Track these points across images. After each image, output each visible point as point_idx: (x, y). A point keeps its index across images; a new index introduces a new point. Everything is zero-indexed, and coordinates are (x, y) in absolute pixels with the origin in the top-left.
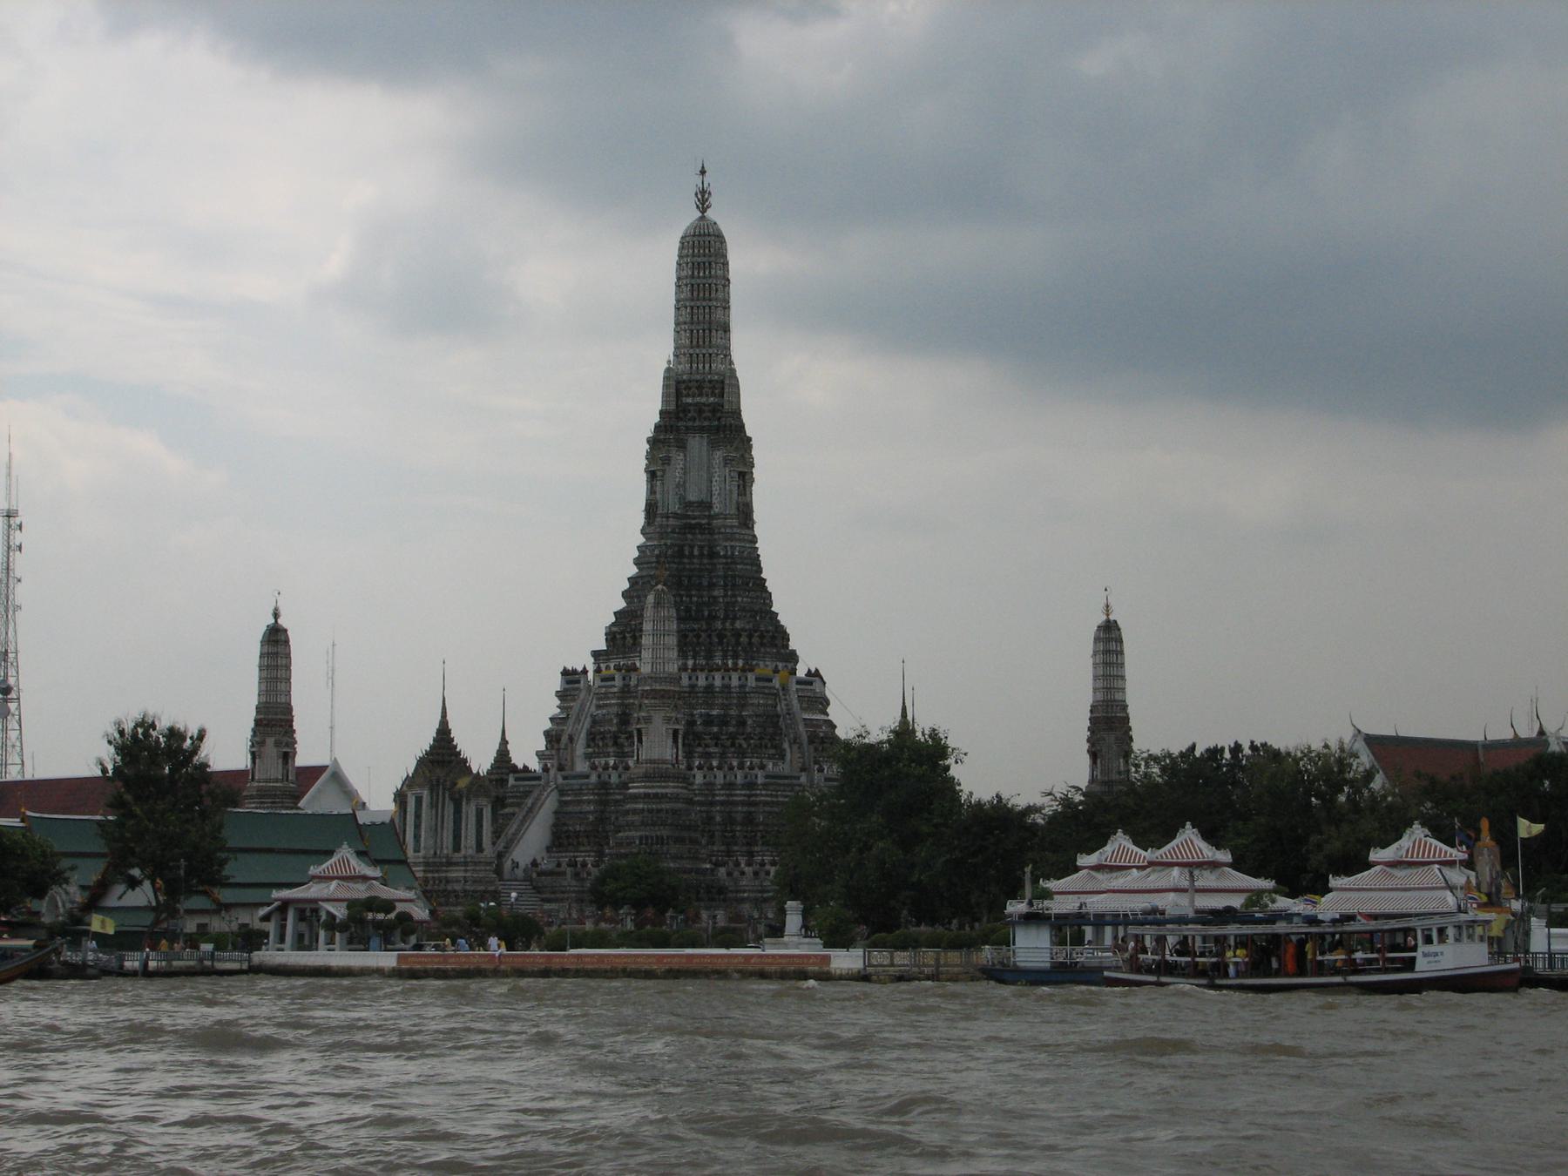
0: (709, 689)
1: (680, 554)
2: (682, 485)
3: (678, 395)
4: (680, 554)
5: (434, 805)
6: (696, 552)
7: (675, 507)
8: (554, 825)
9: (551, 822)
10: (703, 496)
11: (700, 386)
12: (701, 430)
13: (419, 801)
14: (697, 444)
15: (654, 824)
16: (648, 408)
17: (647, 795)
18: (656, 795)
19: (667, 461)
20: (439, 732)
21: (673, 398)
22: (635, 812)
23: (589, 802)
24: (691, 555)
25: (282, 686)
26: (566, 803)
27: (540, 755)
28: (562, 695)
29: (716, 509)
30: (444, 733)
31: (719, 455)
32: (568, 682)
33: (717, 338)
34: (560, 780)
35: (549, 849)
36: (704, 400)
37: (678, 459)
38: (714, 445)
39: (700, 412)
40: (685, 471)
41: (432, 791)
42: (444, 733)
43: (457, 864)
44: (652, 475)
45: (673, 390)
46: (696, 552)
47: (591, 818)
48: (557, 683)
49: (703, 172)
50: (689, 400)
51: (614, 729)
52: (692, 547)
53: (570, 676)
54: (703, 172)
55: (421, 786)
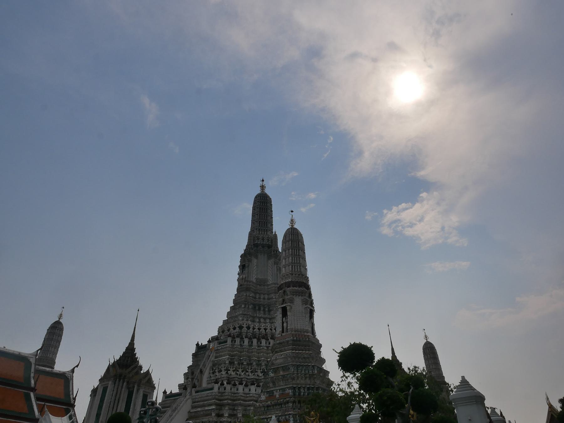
16: (241, 244)
19: (250, 261)
20: (127, 349)
27: (180, 386)
28: (194, 356)
30: (130, 350)
31: (271, 262)
33: (269, 225)
34: (194, 393)
37: (255, 261)
42: (130, 350)
44: (243, 267)
49: (263, 181)
53: (200, 348)
54: (263, 181)
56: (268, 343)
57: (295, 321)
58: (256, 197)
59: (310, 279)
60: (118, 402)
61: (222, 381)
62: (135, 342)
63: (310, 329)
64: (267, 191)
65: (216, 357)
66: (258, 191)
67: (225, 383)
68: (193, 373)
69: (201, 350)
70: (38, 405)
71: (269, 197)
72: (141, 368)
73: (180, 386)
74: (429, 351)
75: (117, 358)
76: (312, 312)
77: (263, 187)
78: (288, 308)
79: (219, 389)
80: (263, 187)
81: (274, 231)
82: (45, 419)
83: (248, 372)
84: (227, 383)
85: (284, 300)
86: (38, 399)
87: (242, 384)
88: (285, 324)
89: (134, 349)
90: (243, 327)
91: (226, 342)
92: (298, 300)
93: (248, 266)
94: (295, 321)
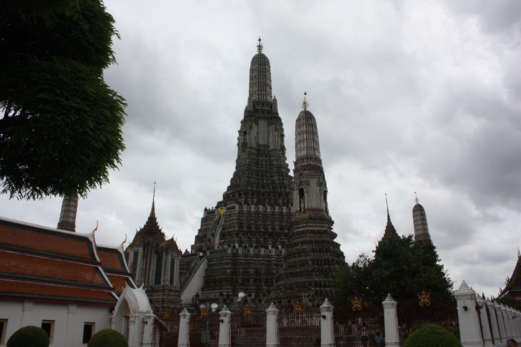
0: (281, 213)
1: (257, 163)
2: (257, 138)
3: (254, 106)
4: (257, 163)
5: (144, 256)
6: (264, 163)
7: (254, 145)
8: (205, 276)
9: (204, 275)
10: (266, 143)
11: (263, 104)
12: (264, 118)
13: (136, 255)
14: (263, 124)
15: (320, 251)
17: (313, 232)
18: (319, 232)
19: (251, 127)
20: (150, 219)
21: (252, 106)
22: (303, 243)
23: (227, 264)
24: (262, 164)
25: (72, 215)
26: (211, 265)
29: (272, 147)
30: (152, 219)
31: (272, 127)
32: (208, 213)
33: (268, 89)
35: (203, 289)
36: (264, 108)
38: (269, 125)
39: (263, 112)
40: (258, 133)
41: (144, 248)
42: (152, 219)
43: (158, 291)
45: (252, 103)
47: (228, 271)
48: (201, 215)
49: (260, 40)
50: (259, 108)
51: (237, 229)
52: (262, 162)
54: (260, 40)
55: (138, 246)
56: (273, 209)
57: (311, 201)
58: (253, 59)
59: (323, 162)
60: (150, 264)
61: (234, 245)
62: (156, 211)
63: (324, 208)
64: (264, 52)
65: (225, 221)
66: (256, 52)
67: (237, 245)
68: (205, 236)
69: (209, 213)
70: (107, 276)
71: (267, 58)
72: (163, 235)
73: (192, 247)
74: (419, 211)
75: (143, 227)
76: (325, 192)
77: (260, 47)
78: (305, 190)
79: (232, 250)
80: (260, 47)
81: (273, 95)
82: (127, 291)
83: (256, 235)
84: (239, 246)
85: (301, 182)
86: (106, 271)
87: (252, 246)
88: (302, 205)
89: (155, 219)
90: (248, 193)
91: (234, 208)
92: (313, 182)
93: (249, 133)
94: (311, 201)
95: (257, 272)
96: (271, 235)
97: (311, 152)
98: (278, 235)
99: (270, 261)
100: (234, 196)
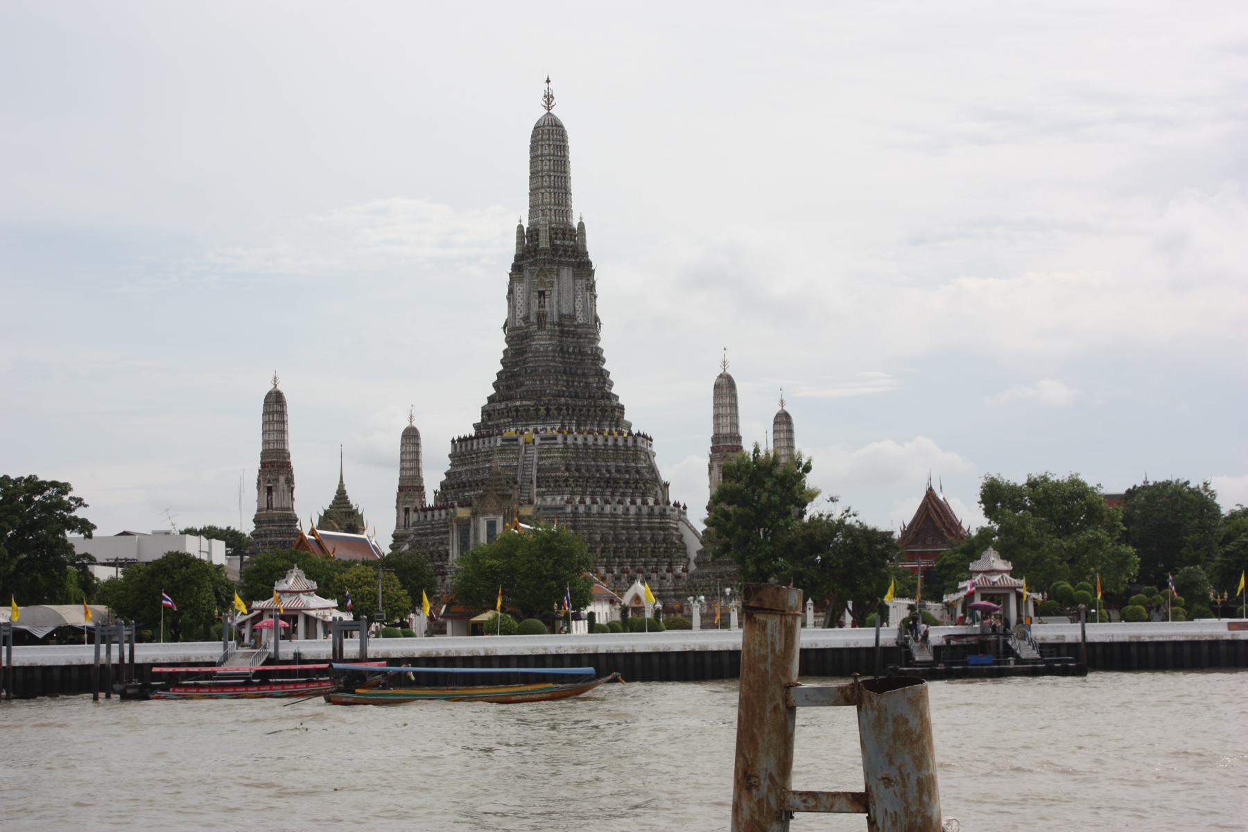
12: (568, 264)
14: (566, 274)
29: (580, 320)
31: (581, 283)
39: (566, 251)
46: (571, 350)
49: (548, 81)
54: (548, 81)
77: (549, 98)
80: (549, 98)
95: (604, 539)
96: (607, 481)
97: (734, 430)
98: (616, 481)
99: (615, 522)
100: (537, 410)
